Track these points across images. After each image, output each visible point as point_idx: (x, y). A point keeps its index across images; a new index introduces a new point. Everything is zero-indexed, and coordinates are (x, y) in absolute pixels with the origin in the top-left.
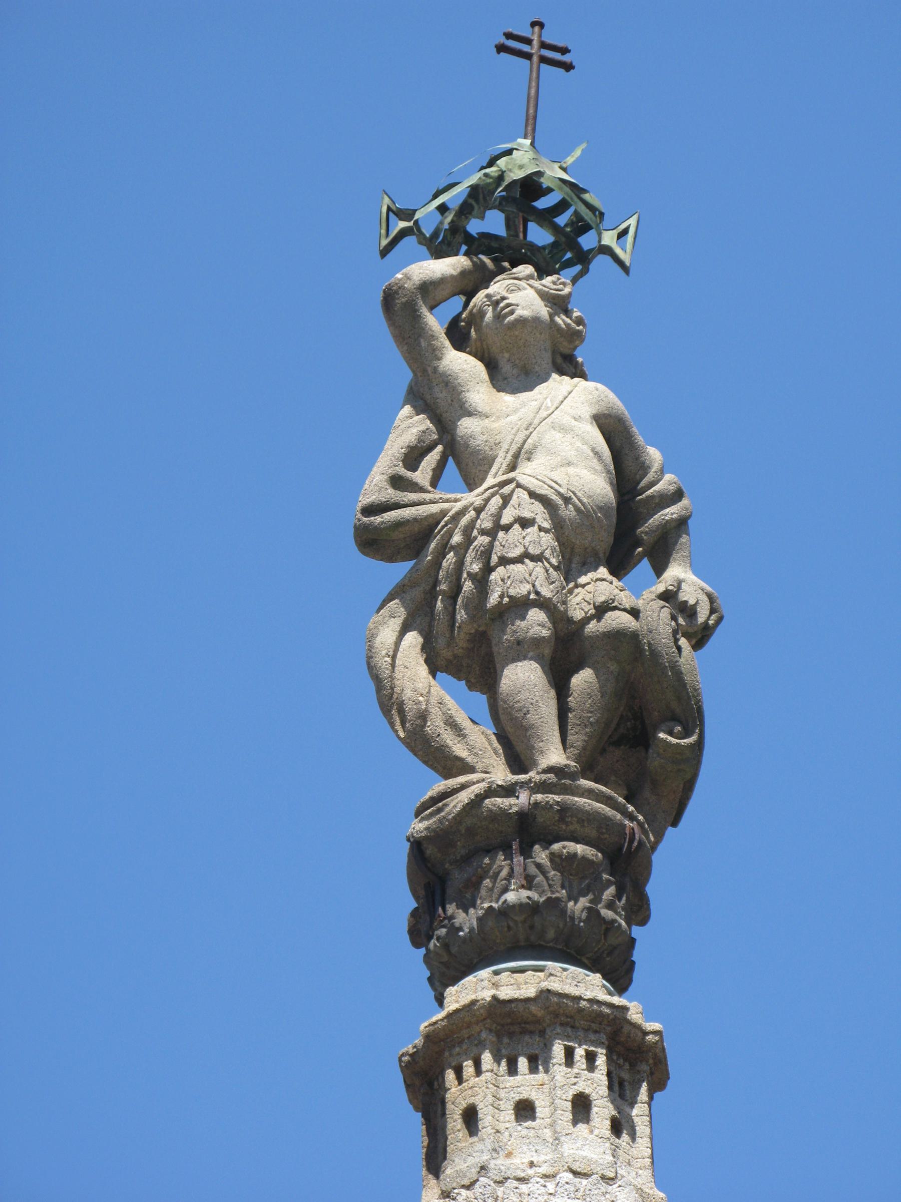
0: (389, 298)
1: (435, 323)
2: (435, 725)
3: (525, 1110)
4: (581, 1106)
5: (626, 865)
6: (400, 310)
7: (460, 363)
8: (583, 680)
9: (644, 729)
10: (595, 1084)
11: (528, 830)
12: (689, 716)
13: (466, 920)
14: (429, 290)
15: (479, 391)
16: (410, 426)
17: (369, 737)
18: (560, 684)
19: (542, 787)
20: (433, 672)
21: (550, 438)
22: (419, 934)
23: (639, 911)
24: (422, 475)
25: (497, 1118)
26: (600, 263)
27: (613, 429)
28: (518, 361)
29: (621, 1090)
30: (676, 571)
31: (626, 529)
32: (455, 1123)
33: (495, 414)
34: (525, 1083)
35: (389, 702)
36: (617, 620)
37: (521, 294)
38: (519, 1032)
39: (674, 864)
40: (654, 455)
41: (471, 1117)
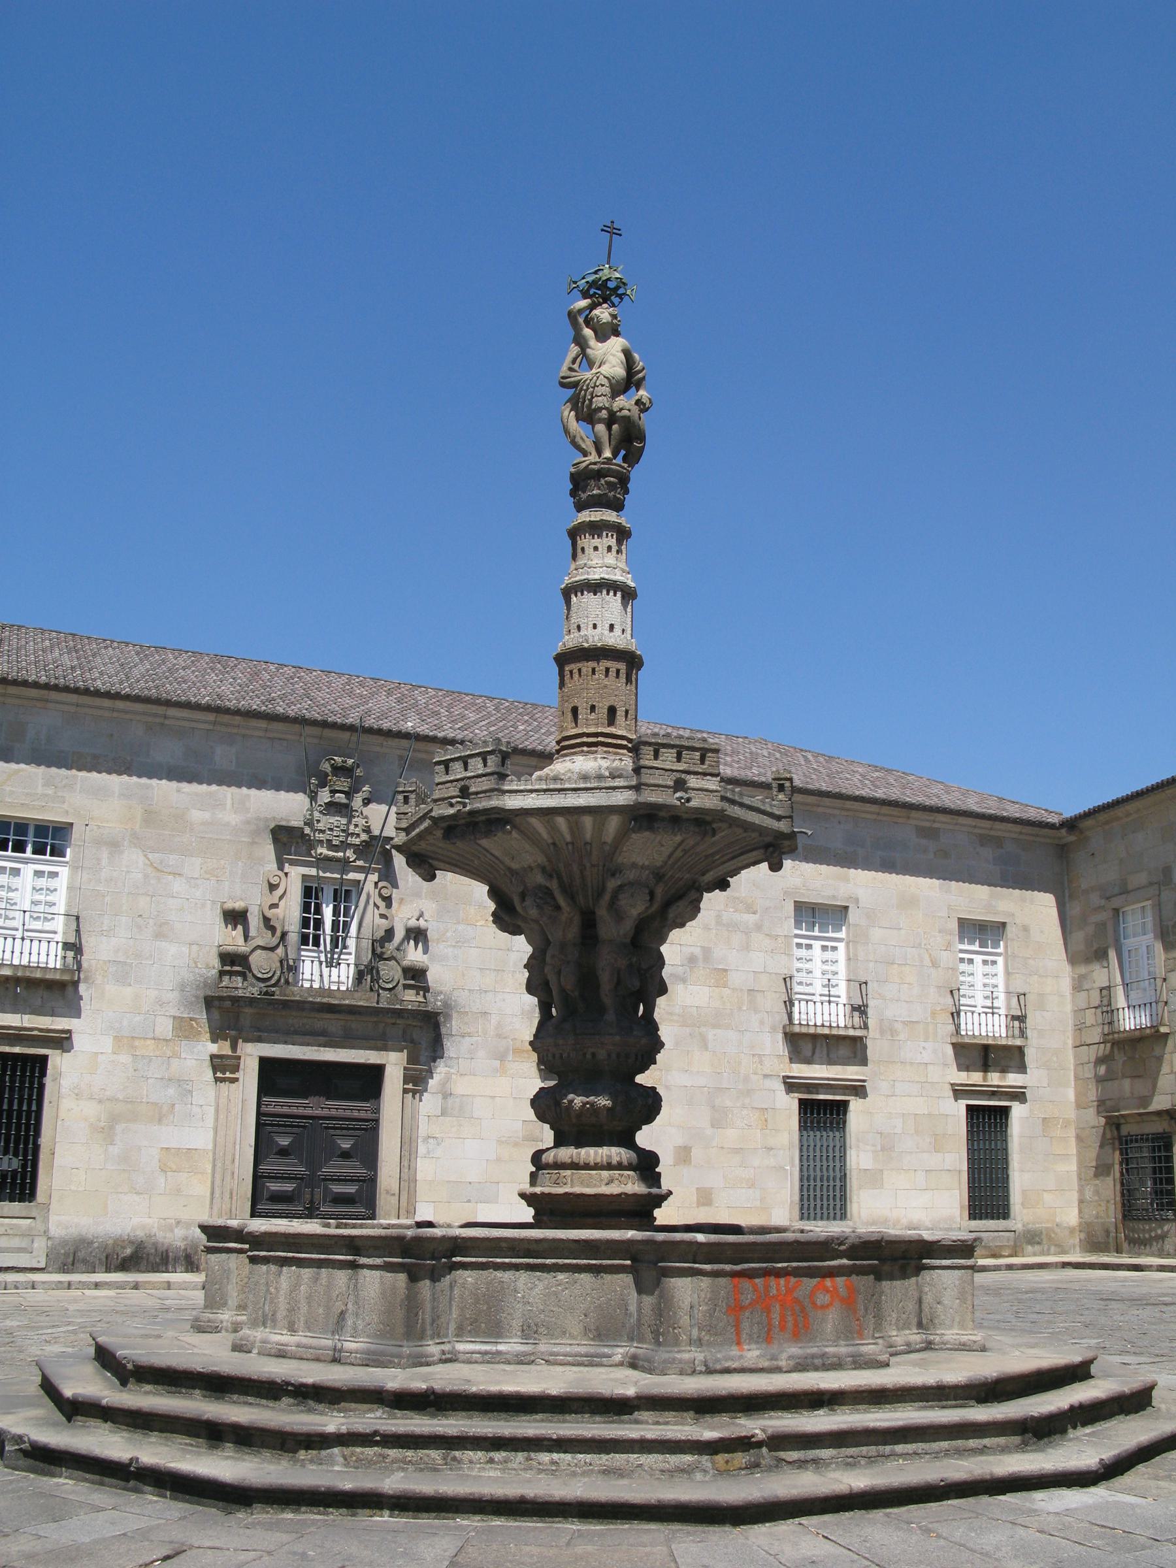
0: (570, 313)
1: (581, 320)
2: (578, 439)
3: (596, 549)
4: (609, 548)
5: (623, 481)
6: (572, 316)
7: (588, 332)
8: (615, 427)
9: (630, 439)
10: (613, 542)
11: (599, 474)
12: (642, 438)
13: (584, 496)
14: (580, 311)
15: (593, 342)
16: (574, 350)
17: (563, 444)
18: (609, 428)
19: (604, 463)
20: (577, 420)
21: (610, 356)
22: (573, 493)
23: (627, 492)
24: (576, 366)
25: (589, 551)
26: (626, 299)
27: (627, 353)
28: (605, 332)
29: (619, 542)
30: (642, 392)
31: (630, 381)
32: (579, 550)
33: (597, 349)
34: (596, 541)
35: (566, 431)
36: (625, 412)
37: (603, 314)
38: (596, 529)
39: (638, 475)
40: (636, 356)
41: (583, 549)
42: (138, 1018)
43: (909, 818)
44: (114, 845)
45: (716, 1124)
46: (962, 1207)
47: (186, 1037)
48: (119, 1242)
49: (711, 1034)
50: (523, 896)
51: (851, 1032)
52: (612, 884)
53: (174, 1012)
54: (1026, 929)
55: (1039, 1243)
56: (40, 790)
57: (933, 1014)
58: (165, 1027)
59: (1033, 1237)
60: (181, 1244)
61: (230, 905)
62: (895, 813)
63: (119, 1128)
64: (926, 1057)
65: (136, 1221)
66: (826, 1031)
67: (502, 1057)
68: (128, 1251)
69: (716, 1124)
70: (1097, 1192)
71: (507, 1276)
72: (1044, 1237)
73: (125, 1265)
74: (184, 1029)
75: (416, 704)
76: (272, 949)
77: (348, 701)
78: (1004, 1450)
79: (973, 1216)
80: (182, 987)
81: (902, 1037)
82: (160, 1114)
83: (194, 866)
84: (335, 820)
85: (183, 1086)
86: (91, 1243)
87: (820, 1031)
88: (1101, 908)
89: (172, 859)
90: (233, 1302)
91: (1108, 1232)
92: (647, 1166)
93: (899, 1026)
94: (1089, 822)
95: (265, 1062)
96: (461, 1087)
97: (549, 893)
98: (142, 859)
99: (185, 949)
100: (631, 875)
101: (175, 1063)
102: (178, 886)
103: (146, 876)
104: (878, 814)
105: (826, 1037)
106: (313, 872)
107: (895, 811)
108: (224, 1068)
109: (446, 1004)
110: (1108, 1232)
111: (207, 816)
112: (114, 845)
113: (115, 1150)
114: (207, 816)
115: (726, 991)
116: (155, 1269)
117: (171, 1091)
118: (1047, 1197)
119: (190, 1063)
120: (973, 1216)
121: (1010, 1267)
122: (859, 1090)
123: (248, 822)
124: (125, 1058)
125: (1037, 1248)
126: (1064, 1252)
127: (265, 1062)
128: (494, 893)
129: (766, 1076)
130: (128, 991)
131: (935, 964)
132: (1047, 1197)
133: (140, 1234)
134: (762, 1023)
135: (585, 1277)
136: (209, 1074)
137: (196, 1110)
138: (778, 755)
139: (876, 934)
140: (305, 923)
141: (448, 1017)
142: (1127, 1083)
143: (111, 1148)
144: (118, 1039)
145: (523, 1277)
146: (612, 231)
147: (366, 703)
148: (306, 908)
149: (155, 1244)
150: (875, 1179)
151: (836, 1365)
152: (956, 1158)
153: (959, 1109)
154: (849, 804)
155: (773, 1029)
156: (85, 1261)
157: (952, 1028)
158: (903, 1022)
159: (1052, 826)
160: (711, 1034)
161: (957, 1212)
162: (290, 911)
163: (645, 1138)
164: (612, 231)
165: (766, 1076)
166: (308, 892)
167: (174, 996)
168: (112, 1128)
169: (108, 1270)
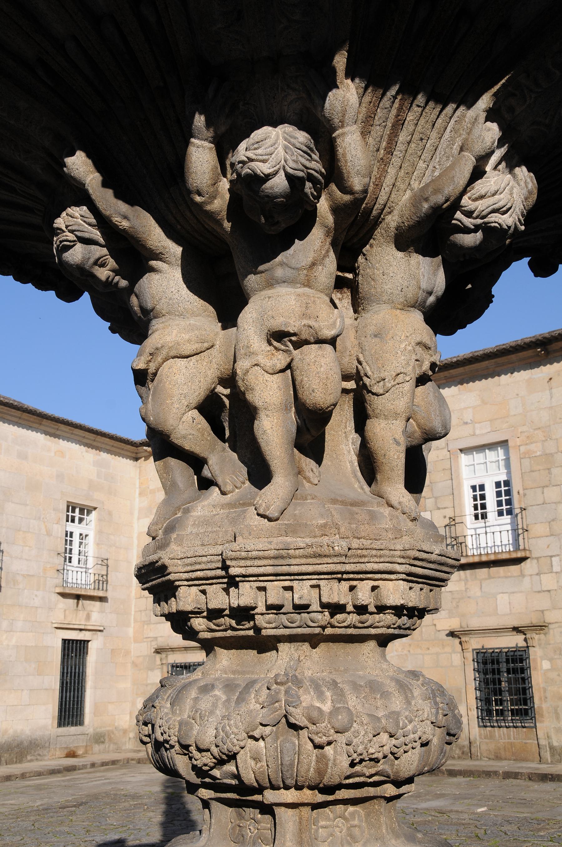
43: (41, 424)
46: (53, 718)
54: (110, 513)
55: (103, 742)
62: (32, 420)
72: (106, 738)
79: (60, 725)
104: (20, 418)
120: (60, 725)
131: (49, 534)
152: (52, 680)
158: (23, 575)
161: (49, 722)
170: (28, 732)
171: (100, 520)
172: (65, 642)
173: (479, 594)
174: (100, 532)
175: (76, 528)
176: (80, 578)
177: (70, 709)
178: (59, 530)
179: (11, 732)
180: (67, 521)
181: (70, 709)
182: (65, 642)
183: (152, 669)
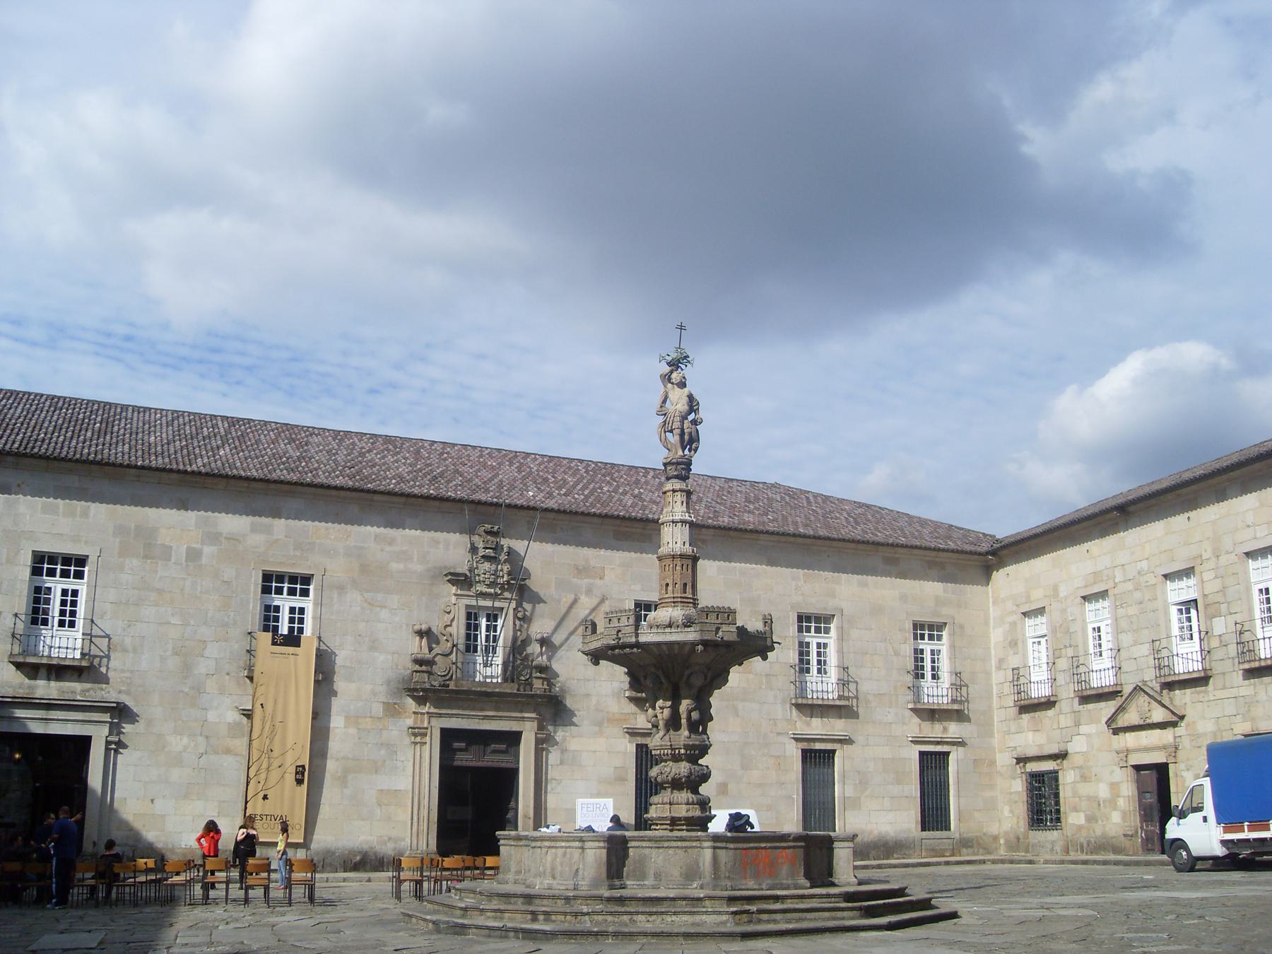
42: (360, 704)
44: (341, 588)
45: (745, 767)
47: (393, 716)
48: (352, 852)
49: (740, 705)
50: (645, 677)
51: (838, 703)
52: (687, 673)
53: (383, 699)
54: (962, 627)
56: (292, 553)
57: (895, 688)
58: (378, 709)
59: (965, 843)
60: (391, 853)
61: (417, 628)
63: (350, 777)
64: (890, 718)
65: (362, 838)
66: (820, 702)
67: (600, 724)
68: (358, 858)
69: (745, 767)
70: (1011, 811)
71: (647, 851)
73: (356, 867)
74: (392, 710)
75: (530, 473)
76: (447, 655)
77: (486, 474)
78: (852, 918)
79: (923, 829)
80: (388, 682)
81: (873, 704)
82: (376, 769)
83: (394, 601)
84: (487, 565)
85: (391, 748)
86: (333, 853)
87: (815, 702)
88: (1013, 612)
89: (380, 596)
90: (513, 870)
91: (1018, 839)
92: (704, 804)
93: (871, 698)
94: (1005, 552)
95: (443, 731)
96: (573, 745)
97: (658, 677)
98: (359, 598)
99: (390, 657)
100: (697, 668)
101: (385, 733)
102: (384, 614)
103: (363, 608)
105: (820, 706)
106: (474, 603)
107: (869, 547)
108: (418, 733)
109: (562, 690)
110: (1018, 839)
111: (401, 566)
112: (341, 588)
113: (347, 792)
114: (401, 566)
115: (751, 676)
116: (376, 869)
117: (383, 752)
118: (977, 815)
119: (395, 733)
120: (923, 829)
121: (947, 863)
122: (847, 741)
123: (428, 570)
124: (352, 731)
125: (970, 850)
126: (989, 853)
127: (443, 731)
128: (629, 674)
129: (779, 734)
130: (353, 686)
131: (897, 654)
132: (977, 815)
133: (365, 847)
134: (775, 697)
135: (679, 851)
136: (408, 740)
137: (399, 764)
138: (787, 498)
139: (855, 633)
140: (468, 637)
141: (564, 697)
142: (1030, 734)
143: (345, 791)
144: (347, 718)
145: (654, 851)
146: (681, 327)
147: (497, 475)
148: (468, 627)
149: (375, 853)
150: (855, 803)
151: (788, 888)
152: (914, 789)
153: (913, 753)
154: (835, 543)
155: (784, 702)
156: (331, 865)
157: (910, 697)
159: (980, 554)
160: (740, 705)
161: (914, 826)
162: (458, 630)
163: (704, 789)
164: (681, 327)
165: (779, 734)
166: (469, 616)
167: (382, 689)
168: (345, 777)
169: (345, 871)
170: (892, 834)
171: (952, 635)
172: (922, 754)
173: (1265, 698)
174: (952, 647)
175: (927, 646)
176: (937, 692)
177: (934, 812)
178: (907, 649)
179: (876, 832)
180: (915, 638)
181: (934, 812)
182: (922, 754)
183: (1014, 778)
